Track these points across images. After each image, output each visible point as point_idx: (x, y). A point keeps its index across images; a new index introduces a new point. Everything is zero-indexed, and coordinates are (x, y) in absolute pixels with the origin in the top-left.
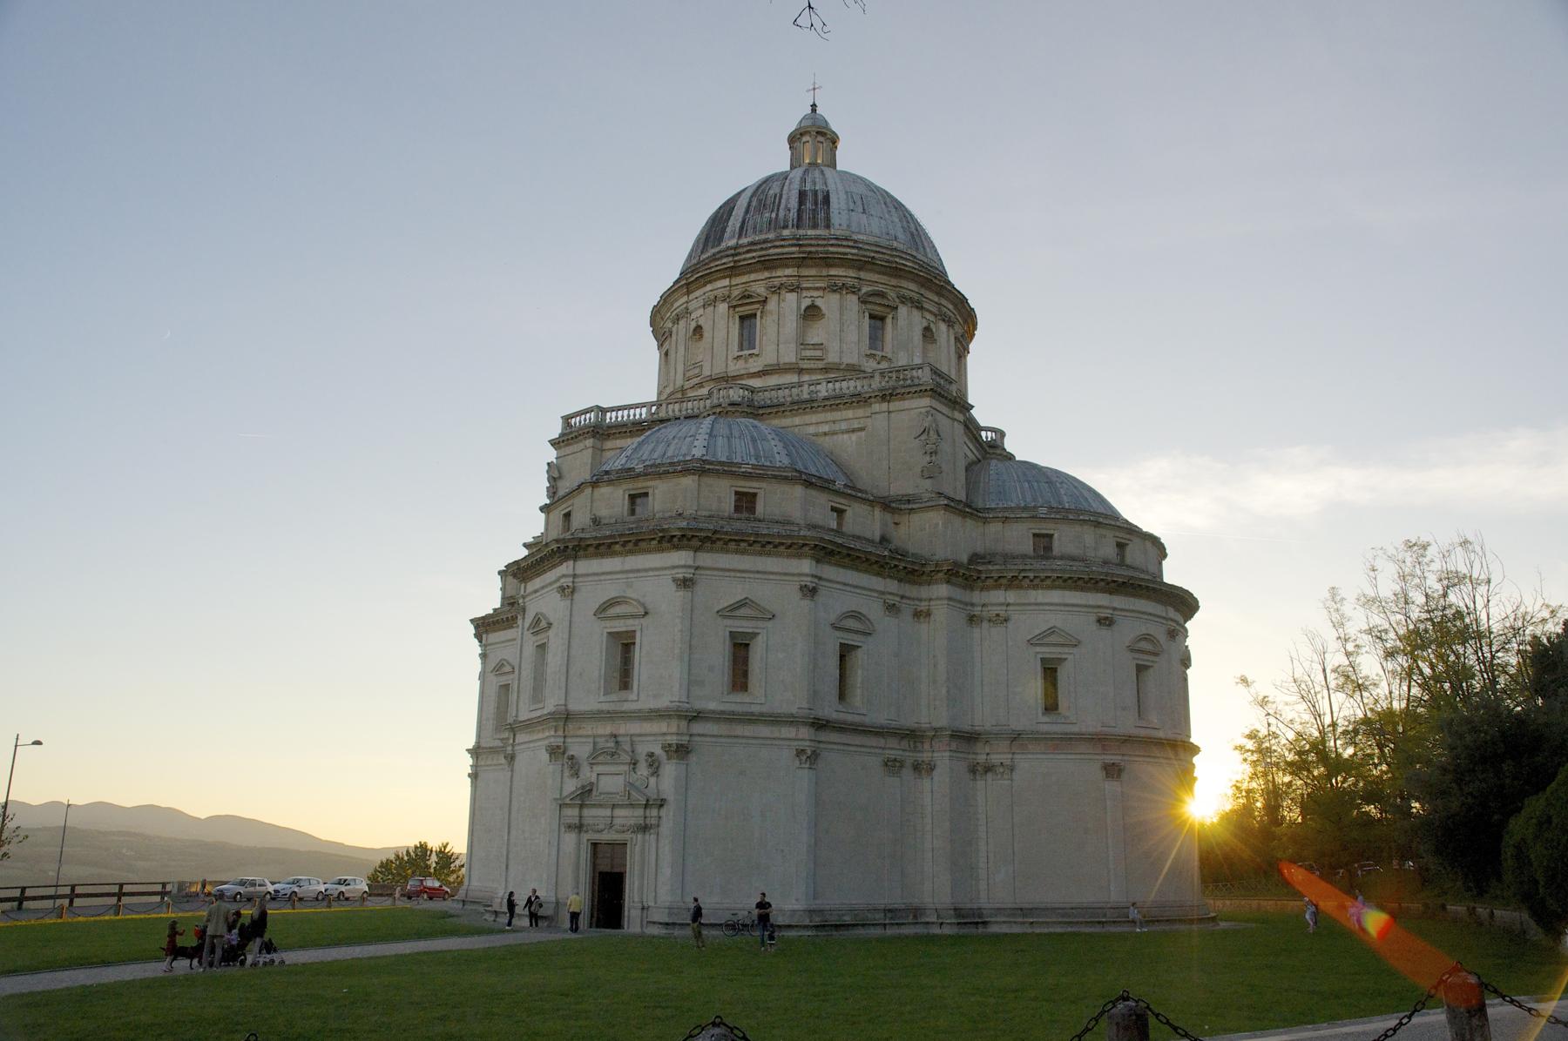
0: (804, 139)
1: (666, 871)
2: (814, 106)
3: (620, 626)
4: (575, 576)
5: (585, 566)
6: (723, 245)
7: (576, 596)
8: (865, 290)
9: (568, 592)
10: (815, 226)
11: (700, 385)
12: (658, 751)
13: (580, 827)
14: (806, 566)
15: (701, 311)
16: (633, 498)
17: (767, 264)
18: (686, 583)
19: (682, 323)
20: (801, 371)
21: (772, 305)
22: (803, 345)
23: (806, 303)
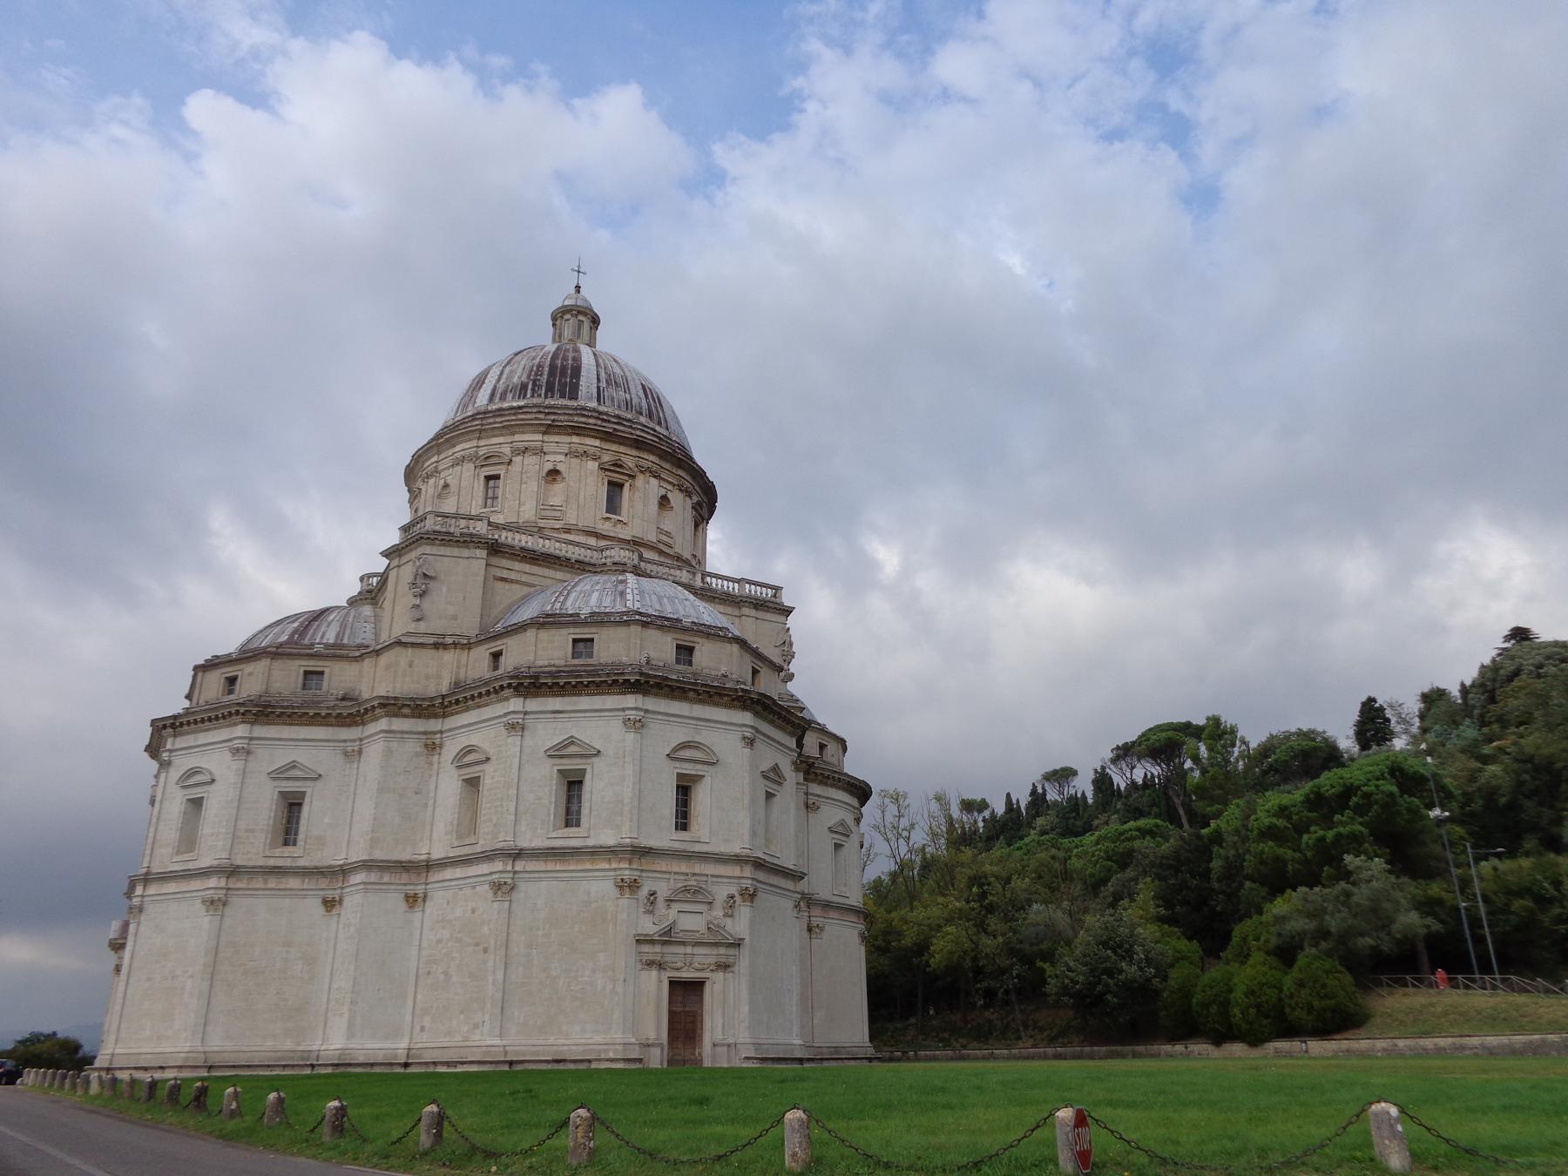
0: (581, 317)
1: (745, 1009)
2: (578, 288)
3: (689, 769)
4: (647, 711)
5: (651, 703)
6: (582, 403)
7: (644, 731)
8: (695, 499)
9: (637, 725)
10: (659, 423)
11: (568, 531)
12: (738, 898)
13: (661, 966)
14: (792, 743)
15: (562, 458)
16: (679, 647)
17: (638, 444)
18: (750, 742)
19: (530, 460)
20: (661, 553)
21: (640, 480)
22: (660, 531)
23: (663, 492)
